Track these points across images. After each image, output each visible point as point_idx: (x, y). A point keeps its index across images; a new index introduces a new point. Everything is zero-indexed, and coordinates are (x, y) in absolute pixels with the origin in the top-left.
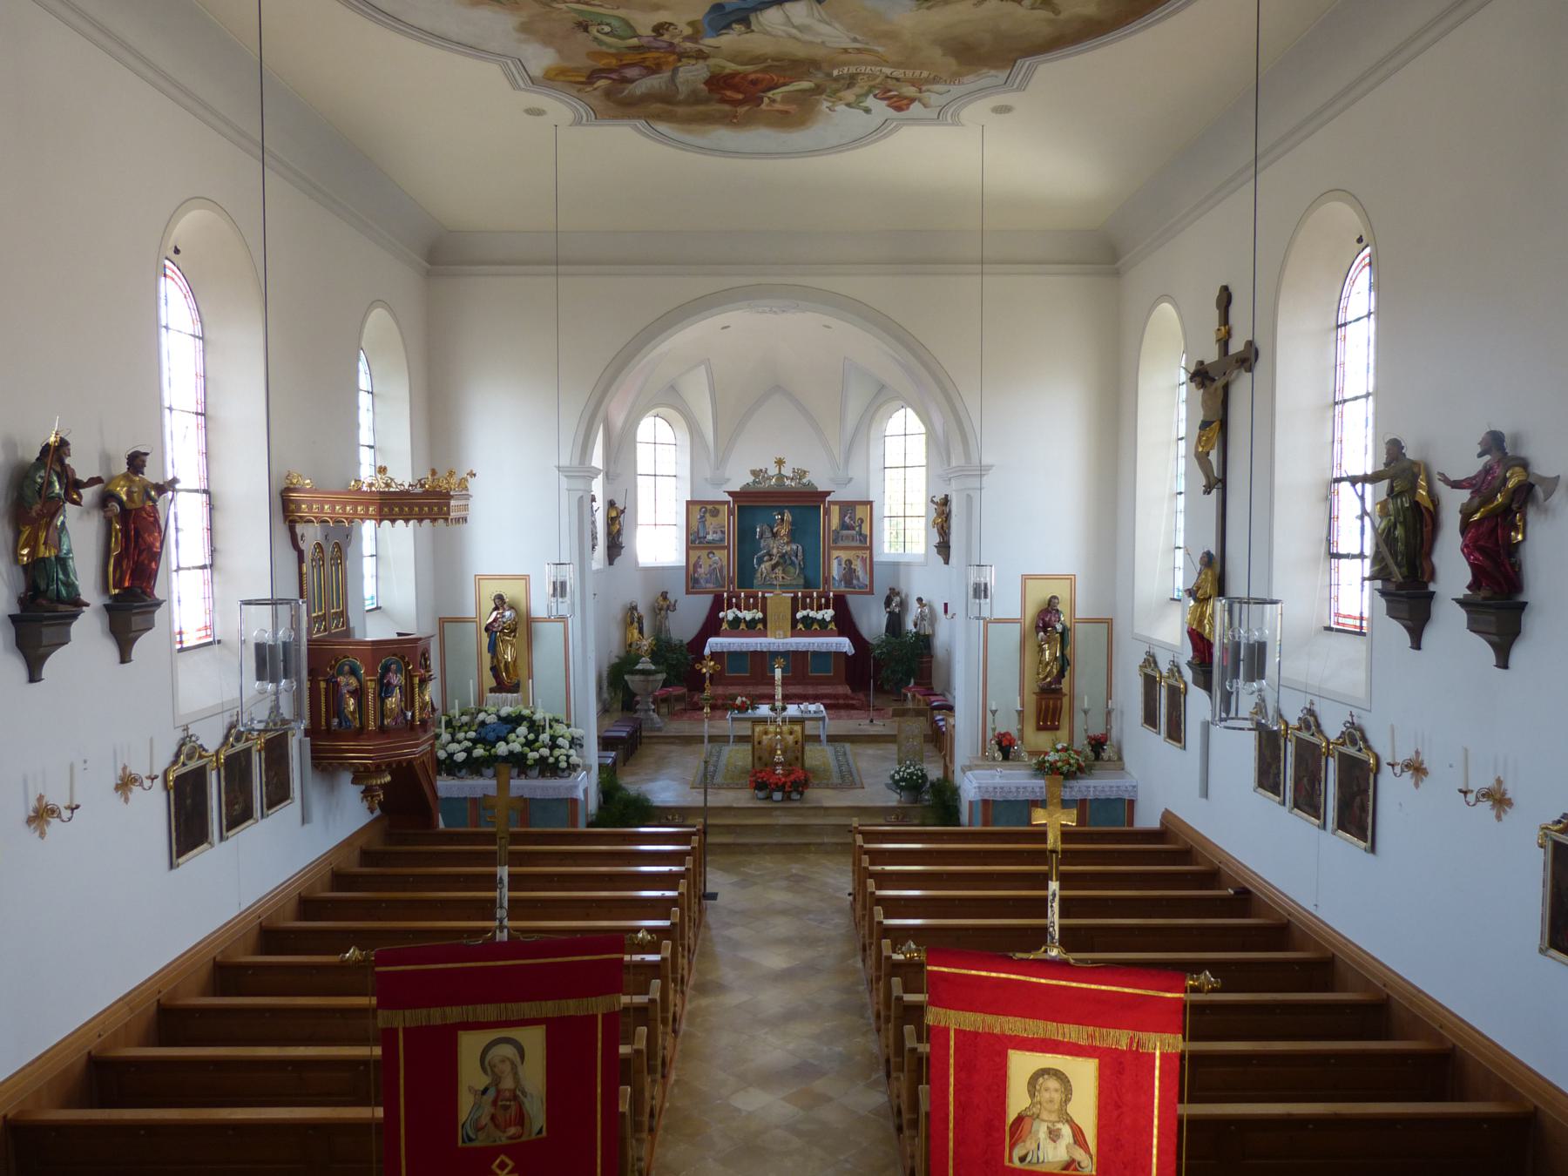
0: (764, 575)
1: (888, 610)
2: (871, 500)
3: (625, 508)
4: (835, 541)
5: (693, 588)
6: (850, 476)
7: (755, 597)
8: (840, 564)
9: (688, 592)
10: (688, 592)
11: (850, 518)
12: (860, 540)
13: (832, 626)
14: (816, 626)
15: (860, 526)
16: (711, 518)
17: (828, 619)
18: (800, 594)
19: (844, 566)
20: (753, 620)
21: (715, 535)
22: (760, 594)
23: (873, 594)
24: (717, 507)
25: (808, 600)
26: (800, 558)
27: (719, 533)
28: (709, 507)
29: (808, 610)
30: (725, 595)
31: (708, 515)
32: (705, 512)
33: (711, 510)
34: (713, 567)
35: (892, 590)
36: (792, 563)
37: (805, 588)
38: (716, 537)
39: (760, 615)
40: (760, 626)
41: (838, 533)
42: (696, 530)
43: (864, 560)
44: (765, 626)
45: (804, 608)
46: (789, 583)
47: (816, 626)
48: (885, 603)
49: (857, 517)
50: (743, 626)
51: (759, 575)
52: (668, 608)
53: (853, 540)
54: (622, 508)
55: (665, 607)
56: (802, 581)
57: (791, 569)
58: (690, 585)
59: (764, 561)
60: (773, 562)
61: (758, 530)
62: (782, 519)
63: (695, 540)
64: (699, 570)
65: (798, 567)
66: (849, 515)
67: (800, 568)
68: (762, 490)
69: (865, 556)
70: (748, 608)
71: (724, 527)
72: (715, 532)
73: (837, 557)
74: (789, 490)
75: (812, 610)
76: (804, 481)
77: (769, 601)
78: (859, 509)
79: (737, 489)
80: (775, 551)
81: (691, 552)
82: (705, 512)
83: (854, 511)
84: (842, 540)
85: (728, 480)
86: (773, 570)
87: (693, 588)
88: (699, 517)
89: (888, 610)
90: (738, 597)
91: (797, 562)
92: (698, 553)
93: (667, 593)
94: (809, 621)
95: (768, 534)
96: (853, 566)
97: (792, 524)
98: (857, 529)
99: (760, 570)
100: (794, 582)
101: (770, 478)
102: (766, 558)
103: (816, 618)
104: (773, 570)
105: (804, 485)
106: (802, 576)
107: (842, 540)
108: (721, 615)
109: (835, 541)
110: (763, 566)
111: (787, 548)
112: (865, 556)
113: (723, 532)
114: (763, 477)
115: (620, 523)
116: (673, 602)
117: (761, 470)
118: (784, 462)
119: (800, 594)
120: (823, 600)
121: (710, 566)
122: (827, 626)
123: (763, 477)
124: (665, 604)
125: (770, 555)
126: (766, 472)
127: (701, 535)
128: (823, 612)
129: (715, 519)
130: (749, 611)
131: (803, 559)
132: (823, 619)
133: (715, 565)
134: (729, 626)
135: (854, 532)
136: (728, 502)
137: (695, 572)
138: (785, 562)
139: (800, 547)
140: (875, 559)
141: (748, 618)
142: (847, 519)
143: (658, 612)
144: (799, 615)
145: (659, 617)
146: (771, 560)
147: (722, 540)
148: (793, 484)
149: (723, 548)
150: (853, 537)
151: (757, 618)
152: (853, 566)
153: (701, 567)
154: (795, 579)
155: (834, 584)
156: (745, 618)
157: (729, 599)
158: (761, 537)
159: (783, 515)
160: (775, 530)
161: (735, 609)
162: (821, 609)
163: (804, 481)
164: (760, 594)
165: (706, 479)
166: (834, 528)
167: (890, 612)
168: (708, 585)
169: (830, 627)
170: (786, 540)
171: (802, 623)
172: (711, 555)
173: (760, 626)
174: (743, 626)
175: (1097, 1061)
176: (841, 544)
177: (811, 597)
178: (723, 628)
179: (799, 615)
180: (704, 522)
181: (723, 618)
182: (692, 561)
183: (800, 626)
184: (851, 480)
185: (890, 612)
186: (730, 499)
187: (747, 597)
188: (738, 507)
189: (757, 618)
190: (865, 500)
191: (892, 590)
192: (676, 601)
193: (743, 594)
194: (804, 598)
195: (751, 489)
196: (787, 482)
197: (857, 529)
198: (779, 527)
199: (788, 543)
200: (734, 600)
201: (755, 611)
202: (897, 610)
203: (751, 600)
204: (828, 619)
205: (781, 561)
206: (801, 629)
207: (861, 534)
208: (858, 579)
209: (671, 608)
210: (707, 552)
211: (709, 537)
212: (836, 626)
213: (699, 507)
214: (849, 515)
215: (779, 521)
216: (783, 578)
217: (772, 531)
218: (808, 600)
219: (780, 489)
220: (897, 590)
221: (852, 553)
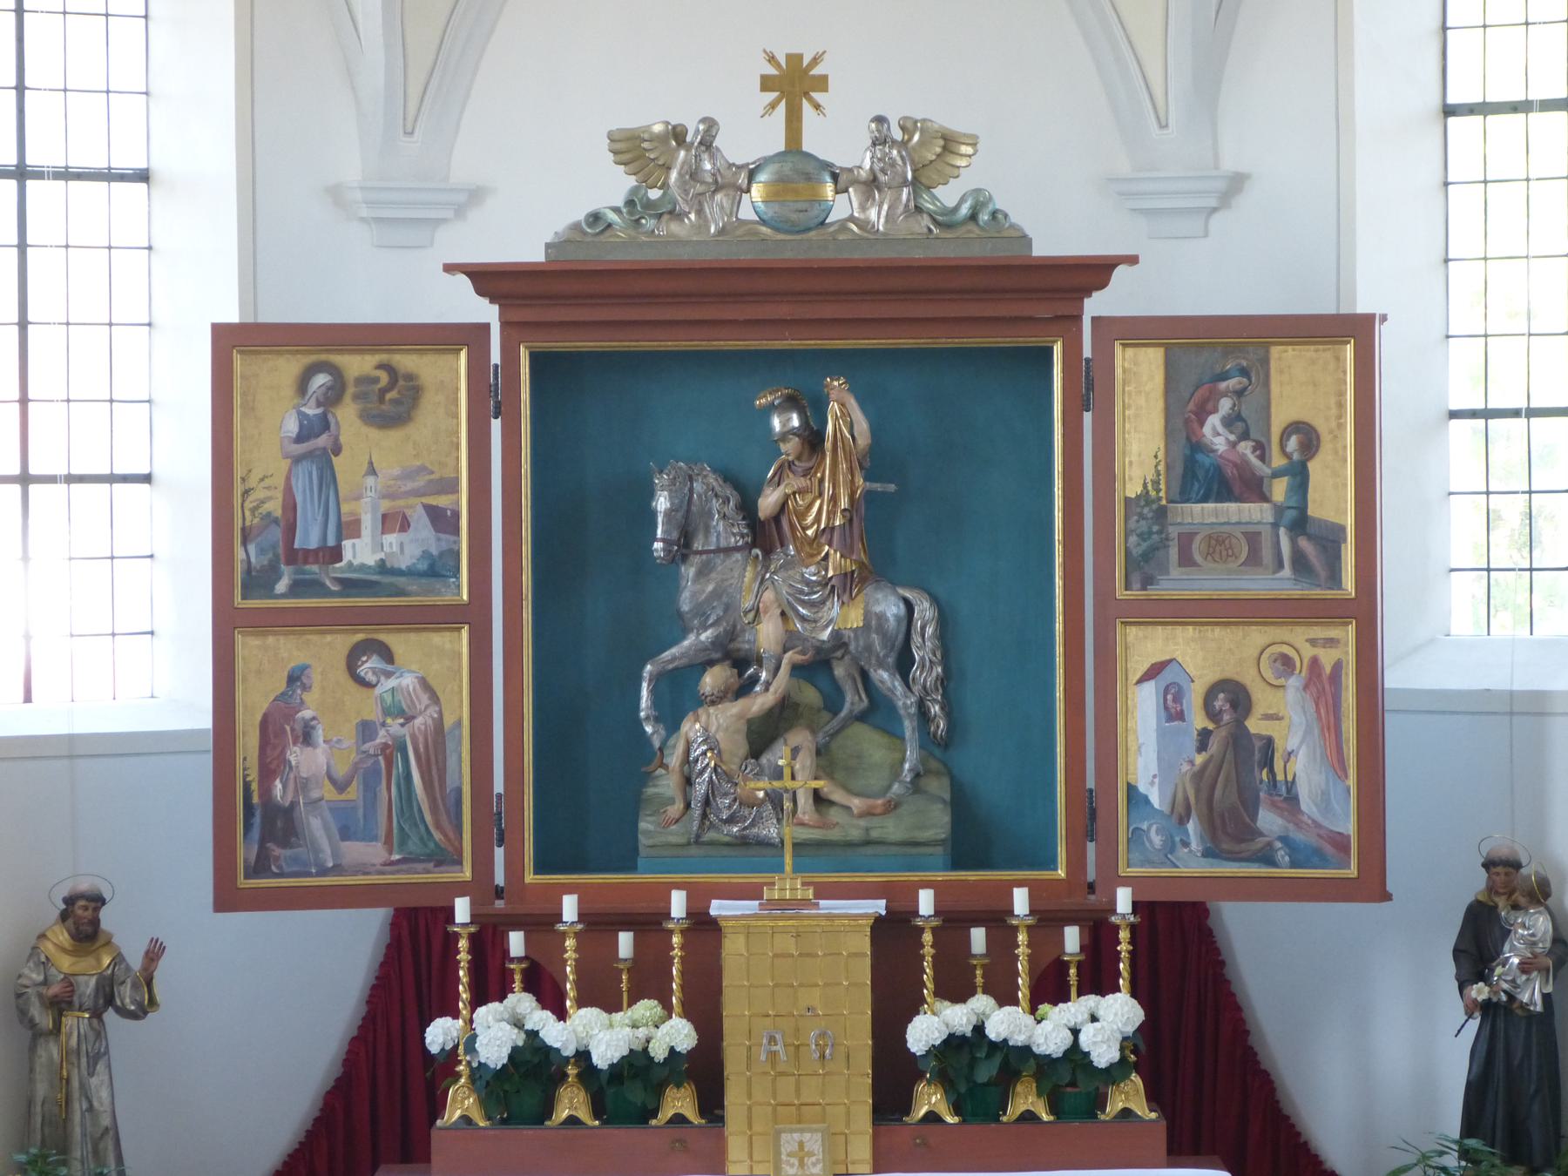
0: (700, 788)
1: (1479, 992)
2: (1362, 308)
4: (1144, 566)
5: (260, 867)
6: (1229, 164)
7: (650, 924)
8: (1173, 712)
9: (227, 898)
10: (227, 898)
11: (1228, 422)
12: (1300, 561)
13: (1130, 1097)
14: (1026, 1100)
15: (1299, 475)
16: (374, 433)
17: (1103, 1053)
18: (926, 902)
19: (1199, 721)
20: (636, 1064)
21: (392, 539)
22: (678, 904)
23: (1386, 897)
24: (407, 362)
25: (978, 938)
26: (926, 674)
27: (420, 519)
28: (357, 365)
29: (981, 1002)
30: (462, 910)
31: (347, 415)
32: (333, 397)
34: (382, 737)
35: (1501, 867)
36: (878, 711)
37: (957, 864)
38: (405, 549)
39: (678, 1034)
40: (680, 1102)
41: (1161, 513)
42: (275, 507)
43: (1322, 684)
44: (712, 1104)
45: (957, 992)
46: (855, 834)
47: (1026, 1100)
48: (1458, 953)
49: (1278, 421)
50: (571, 1103)
51: (667, 784)
52: (107, 995)
53: (1254, 559)
55: (88, 986)
56: (937, 822)
57: (868, 743)
58: (244, 852)
59: (700, 701)
60: (760, 702)
61: (662, 503)
62: (813, 439)
63: (272, 573)
64: (295, 754)
65: (909, 727)
66: (1225, 405)
67: (928, 740)
68: (685, 255)
69: (1327, 658)
70: (603, 996)
71: (451, 486)
72: (394, 521)
73: (1154, 672)
74: (857, 255)
75: (1006, 997)
76: (948, 195)
77: (733, 947)
78: (1288, 361)
79: (530, 250)
80: (767, 634)
81: (247, 646)
82: (333, 397)
83: (1256, 374)
84: (1186, 560)
85: (476, 195)
86: (756, 751)
87: (260, 867)
88: (292, 426)
89: (1479, 992)
90: (542, 924)
91: (905, 702)
92: (289, 650)
93: (98, 901)
94: (986, 1072)
95: (723, 530)
96: (1254, 725)
97: (876, 462)
98: (1280, 490)
99: (674, 760)
100: (891, 828)
101: (734, 182)
102: (711, 680)
103: (1026, 1050)
104: (756, 751)
105: (945, 221)
106: (939, 786)
107: (1186, 560)
108: (440, 1033)
109: (1144, 566)
110: (692, 728)
111: (845, 616)
112: (1327, 658)
113: (443, 521)
114: (694, 174)
116: (135, 961)
117: (678, 134)
118: (822, 83)
119: (926, 902)
120: (1072, 938)
121: (366, 730)
122: (1100, 1102)
123: (694, 174)
124: (87, 973)
125: (742, 661)
126: (707, 144)
127: (309, 537)
128: (1075, 1010)
129: (394, 436)
130: (611, 1006)
131: (944, 681)
132: (1075, 1055)
133: (395, 725)
134: (483, 1103)
135: (1254, 512)
136: (474, 335)
137: (271, 766)
138: (833, 703)
139: (925, 610)
140: (1396, 677)
141: (604, 1054)
142: (1215, 433)
143: (45, 1020)
144: (923, 1033)
145: (50, 1051)
146: (744, 689)
147: (438, 569)
148: (876, 216)
149: (446, 618)
150: (1253, 539)
151: (659, 1052)
152: (1254, 725)
153: (306, 738)
154: (892, 807)
155: (1136, 836)
156: (583, 1056)
157: (488, 938)
158: (683, 545)
159: (812, 406)
160: (768, 502)
161: (521, 1001)
162: (1060, 996)
163: (948, 195)
164: (678, 904)
165: (335, 194)
166: (1134, 490)
167: (1487, 1009)
168: (356, 851)
169: (1115, 1104)
170: (836, 562)
171: (945, 1080)
172: (369, 666)
173: (680, 1102)
174: (571, 1103)
175: (1131, 889)
176: (1175, 584)
177: (998, 920)
178: (453, 1114)
179: (923, 1033)
180: (324, 462)
181: (450, 1057)
182: (253, 701)
183: (930, 1099)
184: (1237, 183)
185: (1487, 1009)
186: (487, 312)
187: (598, 924)
188: (535, 358)
189: (659, 1052)
190: (1328, 308)
191: (1501, 867)
192: (154, 953)
193: (570, 907)
194: (953, 922)
195: (623, 249)
196: (842, 207)
197: (1280, 490)
198: (792, 483)
199: (847, 585)
200: (516, 942)
201: (646, 1008)
202: (1532, 994)
203: (625, 942)
204: (1103, 1053)
205: (810, 695)
206: (932, 1118)
207: (1300, 523)
208: (1289, 800)
209: (126, 995)
210: (341, 642)
211: (360, 552)
212: (1153, 1097)
213: (288, 367)
214: (1225, 405)
215: (790, 448)
216: (818, 798)
217: (748, 508)
218: (978, 938)
219: (792, 250)
220: (1529, 871)
221: (1257, 637)
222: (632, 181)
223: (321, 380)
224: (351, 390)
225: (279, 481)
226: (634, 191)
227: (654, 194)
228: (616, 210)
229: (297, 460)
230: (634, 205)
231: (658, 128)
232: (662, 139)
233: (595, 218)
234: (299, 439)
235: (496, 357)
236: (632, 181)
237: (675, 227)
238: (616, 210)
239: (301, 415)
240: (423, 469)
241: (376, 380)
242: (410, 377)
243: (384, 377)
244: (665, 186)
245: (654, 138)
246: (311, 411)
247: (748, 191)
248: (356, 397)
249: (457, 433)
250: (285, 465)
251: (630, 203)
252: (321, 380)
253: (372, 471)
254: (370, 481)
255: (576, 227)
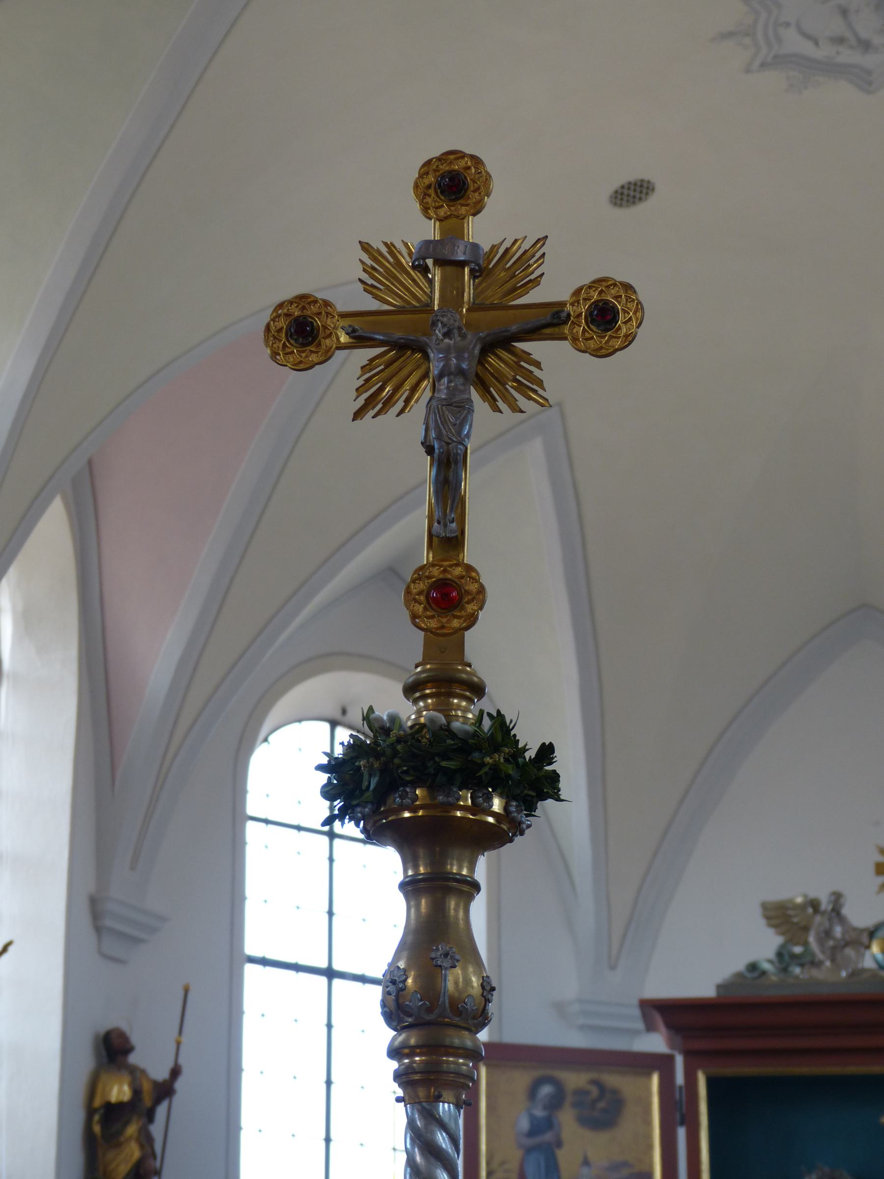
3: (176, 1072)
24: (612, 1080)
28: (575, 1080)
31: (567, 1119)
32: (556, 1103)
33: (580, 1092)
54: (160, 1073)
82: (556, 1103)
88: (524, 1124)
115: (146, 1140)
117: (814, 904)
126: (836, 911)
136: (663, 1063)
165: (560, 1008)
222: (779, 940)
223: (546, 1090)
224: (569, 1099)
225: (514, 1165)
226: (783, 947)
227: (798, 950)
228: (770, 961)
229: (529, 1150)
230: (783, 957)
231: (799, 900)
232: (802, 907)
233: (753, 967)
234: (532, 1133)
235: (680, 1078)
236: (779, 940)
237: (816, 973)
238: (770, 961)
239: (533, 1118)
240: (625, 1164)
241: (587, 1093)
242: (615, 1092)
243: (595, 1091)
244: (806, 944)
245: (797, 907)
246: (539, 1113)
247: (868, 947)
248: (576, 1105)
249: (649, 1136)
250: (518, 1154)
251: (780, 955)
252: (546, 1090)
253: (586, 1162)
254: (585, 1171)
255: (739, 975)
